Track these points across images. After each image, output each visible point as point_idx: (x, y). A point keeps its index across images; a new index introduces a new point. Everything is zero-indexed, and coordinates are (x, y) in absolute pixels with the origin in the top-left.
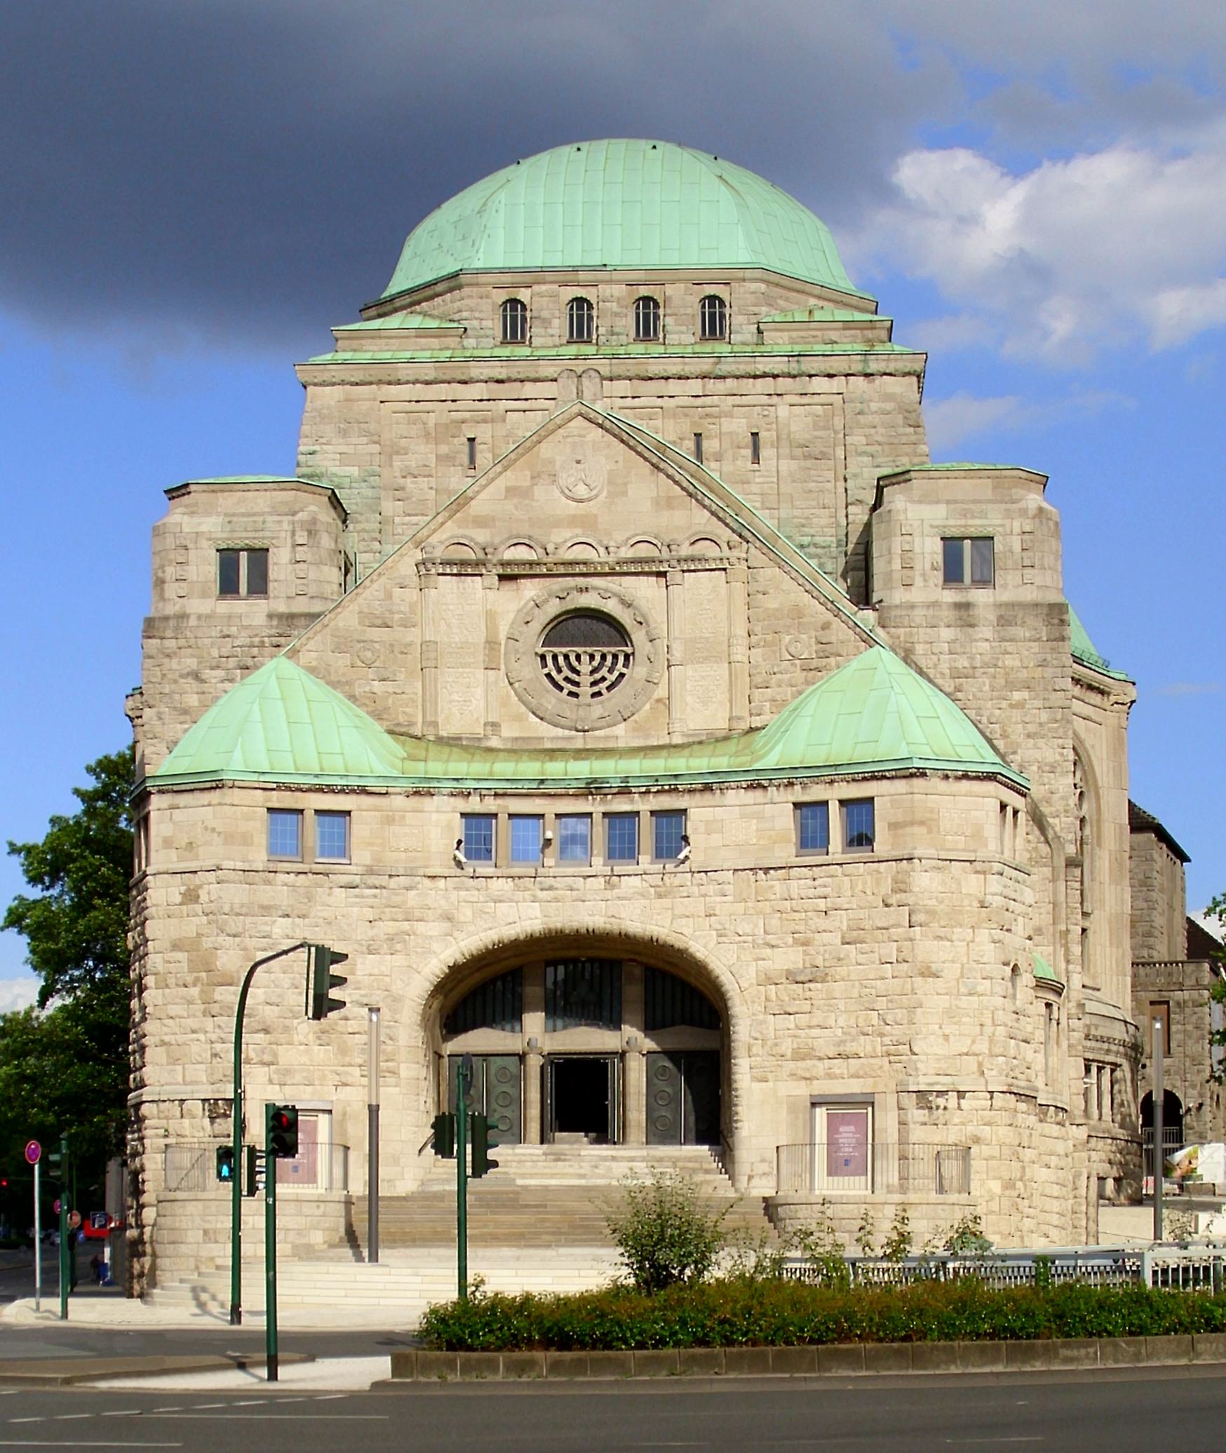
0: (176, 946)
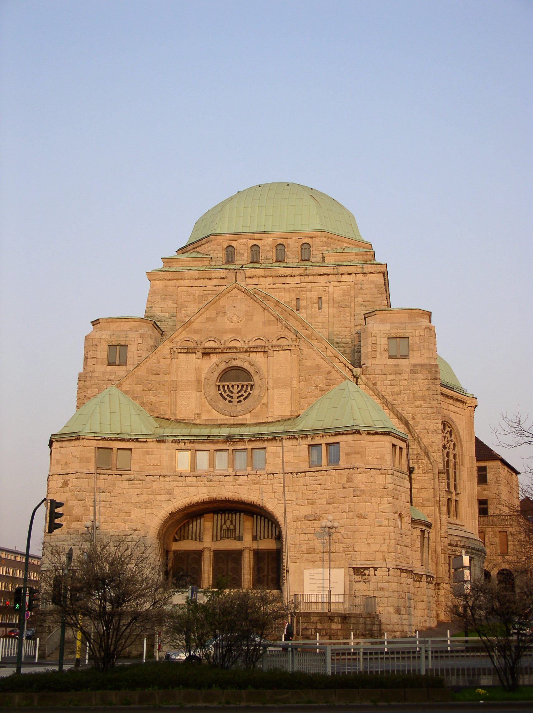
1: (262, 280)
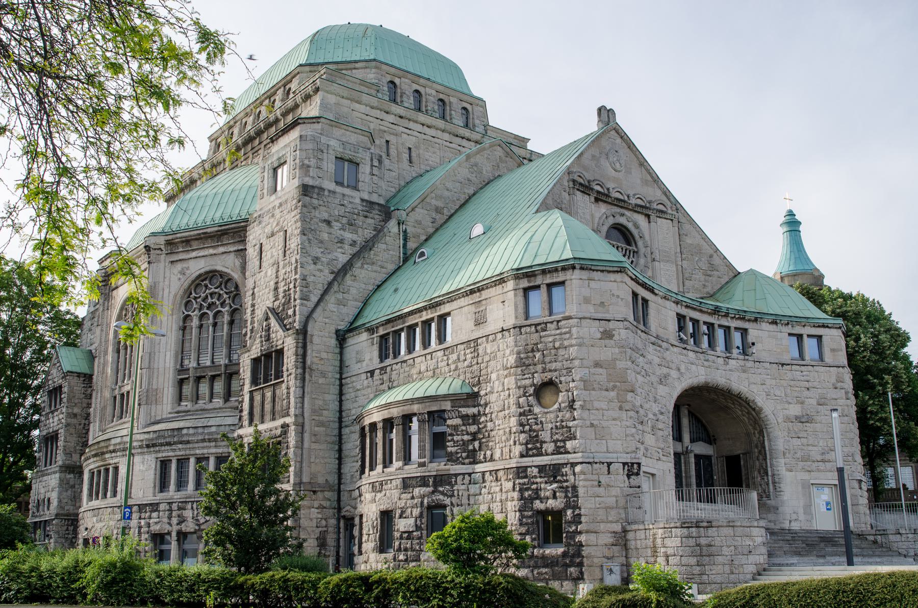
0: (597, 365)
1: (439, 134)
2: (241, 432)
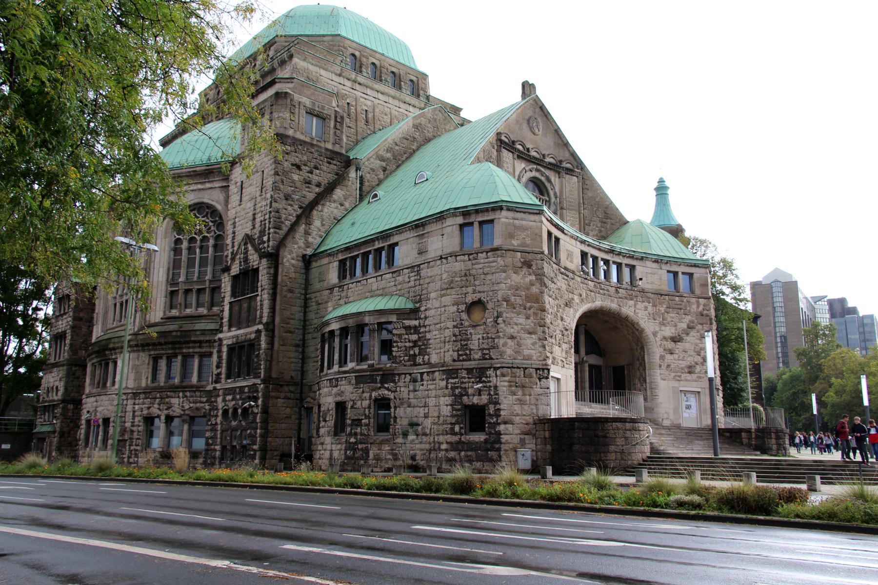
2: (221, 336)
